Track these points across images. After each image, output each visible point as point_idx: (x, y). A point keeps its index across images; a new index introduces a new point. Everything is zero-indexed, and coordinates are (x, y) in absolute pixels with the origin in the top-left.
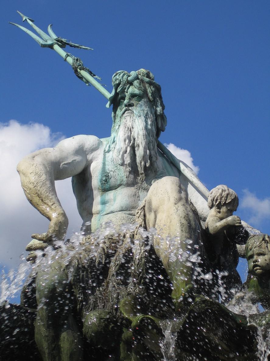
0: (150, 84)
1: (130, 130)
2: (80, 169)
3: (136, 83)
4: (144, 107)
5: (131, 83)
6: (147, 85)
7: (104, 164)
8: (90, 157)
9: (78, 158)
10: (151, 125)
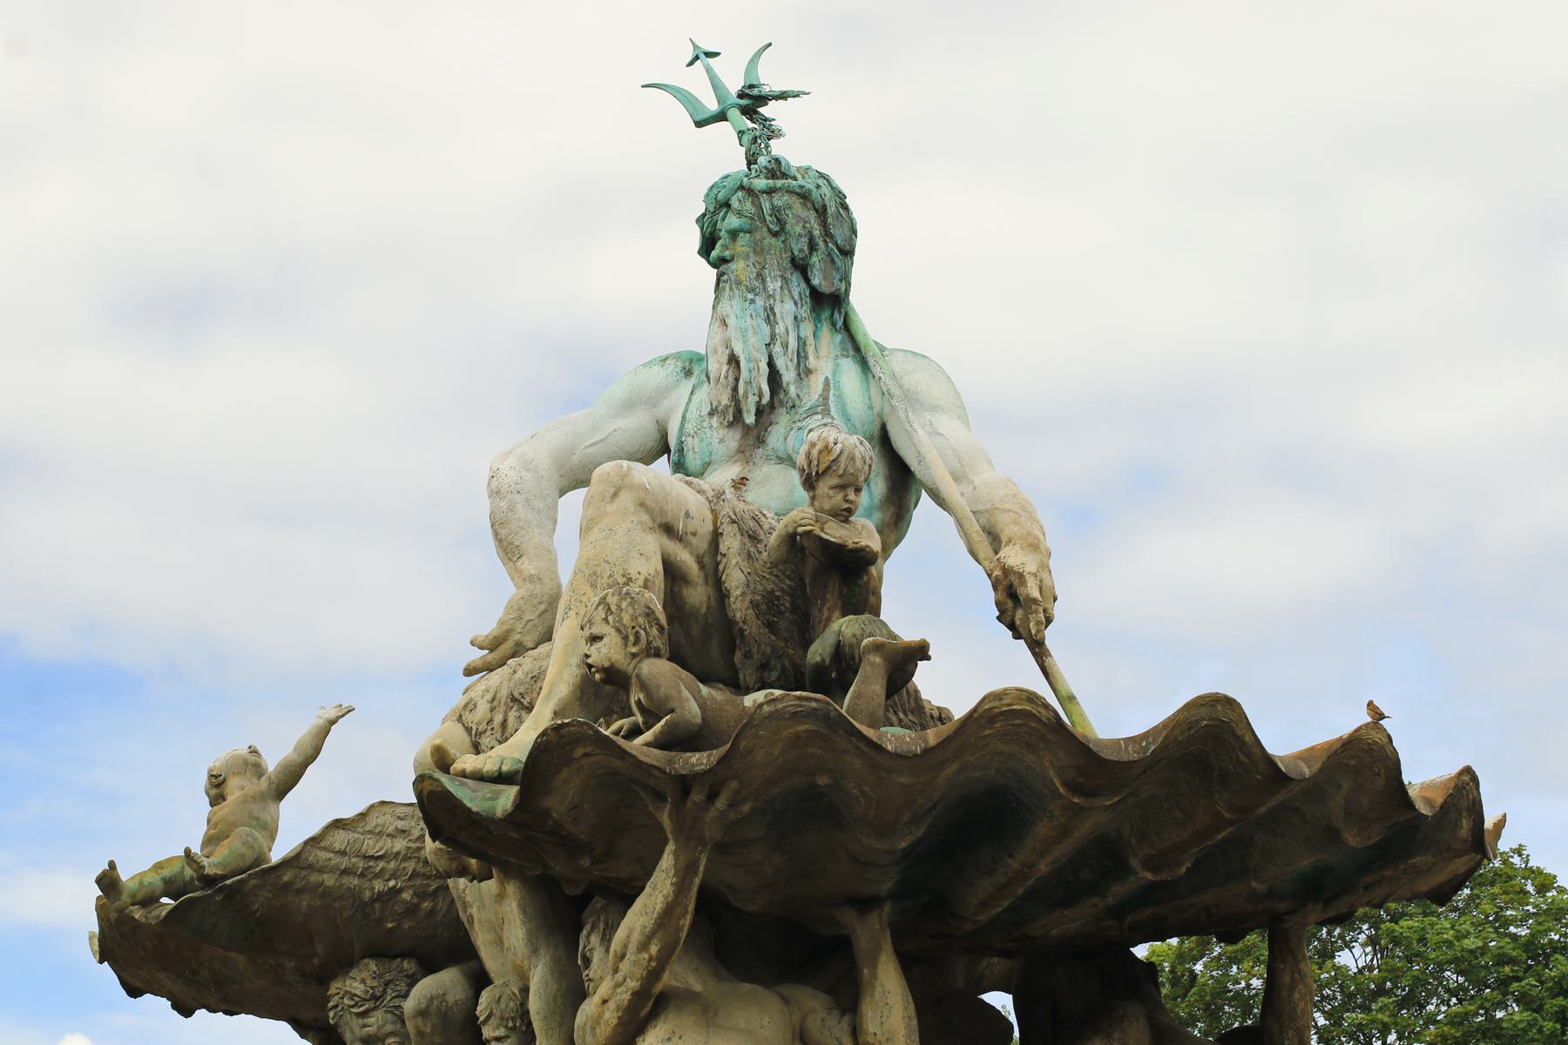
1: (724, 323)
3: (735, 203)
8: (660, 412)
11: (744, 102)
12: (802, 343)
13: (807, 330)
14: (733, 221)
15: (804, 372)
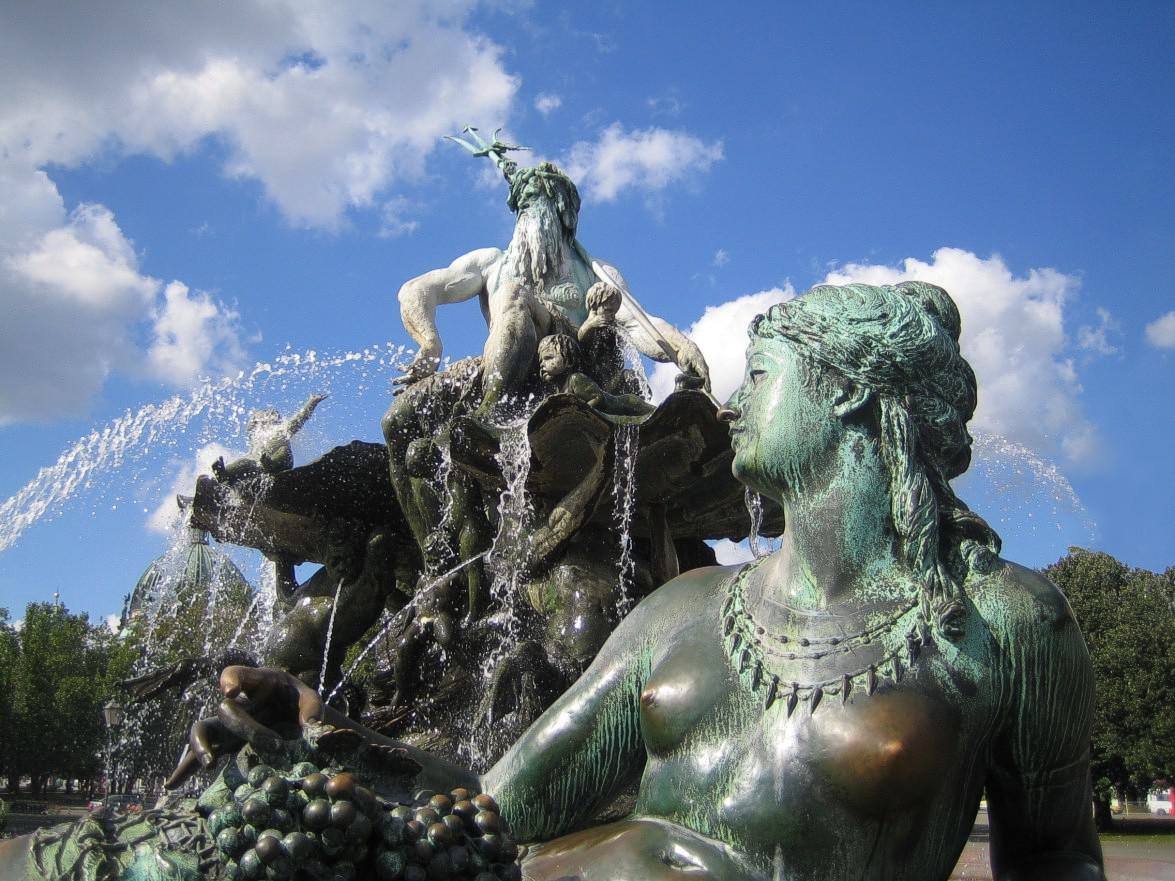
0: (548, 178)
2: (476, 286)
3: (531, 181)
4: (541, 206)
5: (526, 182)
6: (545, 181)
7: (499, 278)
8: (484, 273)
9: (469, 276)
10: (551, 225)
11: (497, 149)
12: (559, 250)
13: (561, 244)
14: (530, 189)
15: (560, 262)
